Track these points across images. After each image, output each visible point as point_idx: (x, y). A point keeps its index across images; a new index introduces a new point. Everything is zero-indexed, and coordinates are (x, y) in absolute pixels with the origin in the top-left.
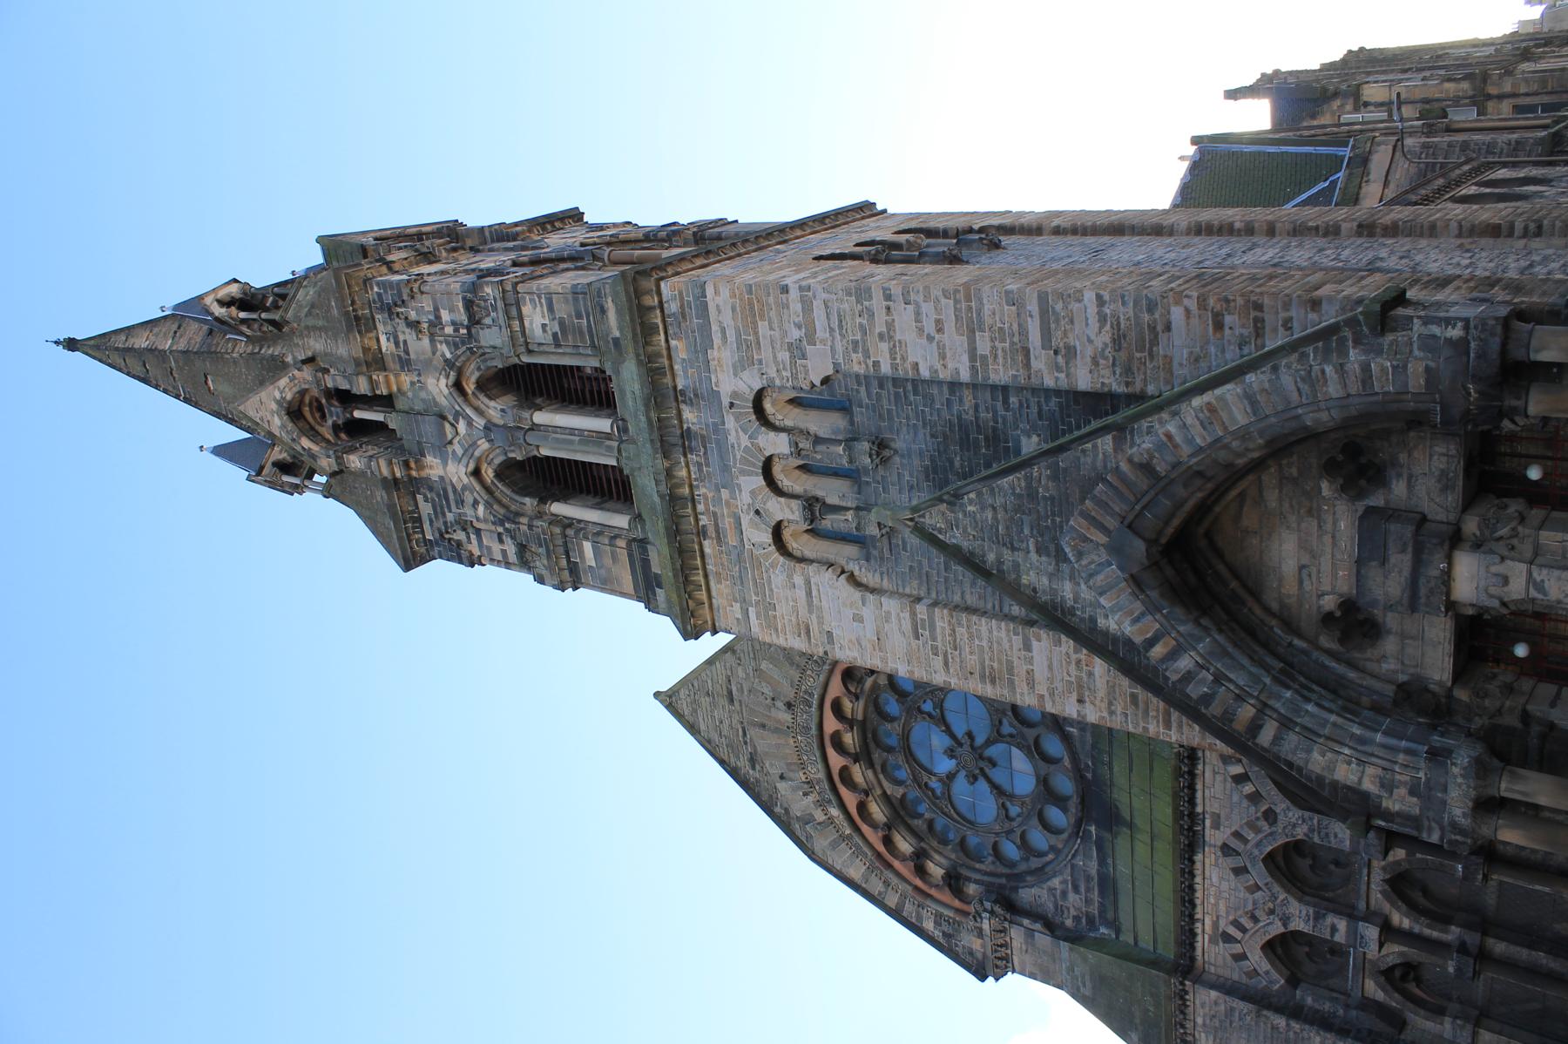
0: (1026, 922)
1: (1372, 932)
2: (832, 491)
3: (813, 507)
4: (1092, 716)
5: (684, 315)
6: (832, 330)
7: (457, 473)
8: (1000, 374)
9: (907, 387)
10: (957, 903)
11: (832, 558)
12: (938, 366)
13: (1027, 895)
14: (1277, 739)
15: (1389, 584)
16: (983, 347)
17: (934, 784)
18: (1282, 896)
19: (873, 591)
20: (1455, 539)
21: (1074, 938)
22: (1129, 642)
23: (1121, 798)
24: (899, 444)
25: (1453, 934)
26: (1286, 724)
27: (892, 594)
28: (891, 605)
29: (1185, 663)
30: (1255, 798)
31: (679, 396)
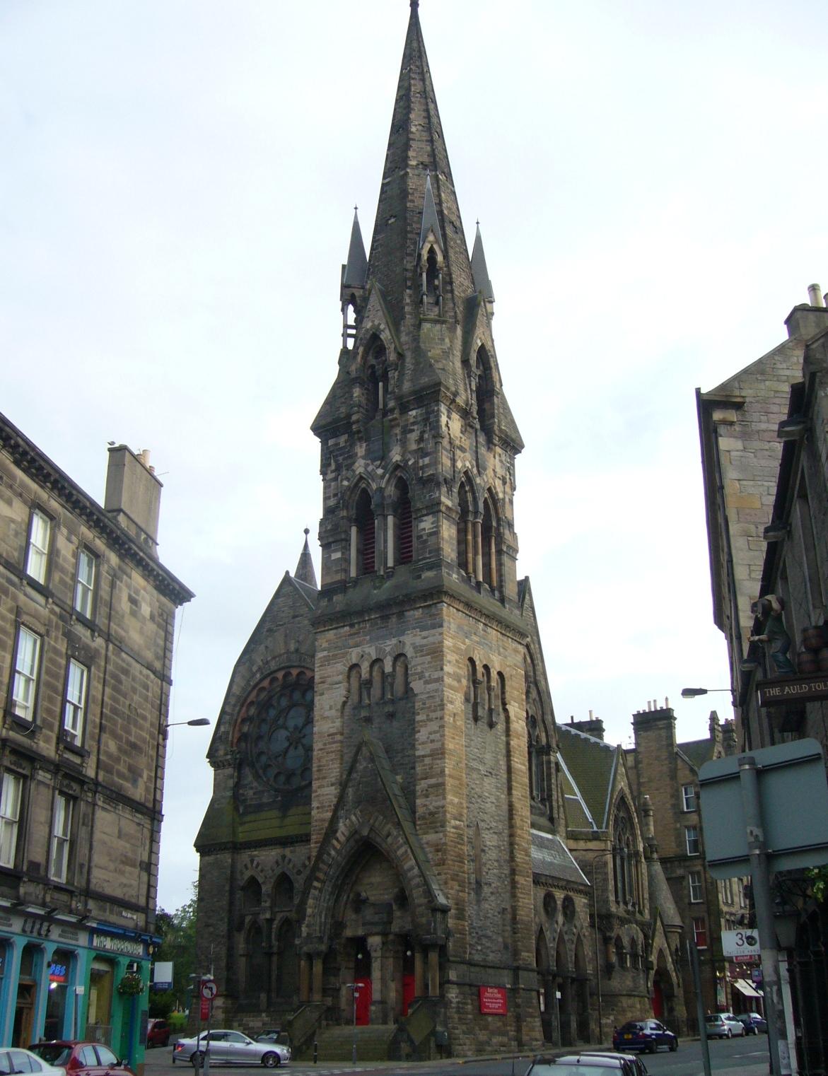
0: (236, 774)
1: (268, 916)
2: (376, 691)
3: (368, 684)
4: (314, 813)
5: (430, 616)
6: (428, 693)
7: (360, 467)
8: (419, 769)
9: (412, 728)
10: (235, 741)
11: (352, 691)
12: (420, 741)
13: (247, 771)
14: (315, 888)
15: (369, 914)
16: (427, 761)
17: (281, 722)
18: (272, 880)
19: (342, 713)
20: (384, 934)
21: (236, 797)
22: (336, 831)
23: (292, 811)
24: (395, 724)
25: (275, 943)
26: (320, 890)
27: (343, 722)
28: (338, 723)
29: (333, 853)
30: (304, 866)
31: (401, 615)
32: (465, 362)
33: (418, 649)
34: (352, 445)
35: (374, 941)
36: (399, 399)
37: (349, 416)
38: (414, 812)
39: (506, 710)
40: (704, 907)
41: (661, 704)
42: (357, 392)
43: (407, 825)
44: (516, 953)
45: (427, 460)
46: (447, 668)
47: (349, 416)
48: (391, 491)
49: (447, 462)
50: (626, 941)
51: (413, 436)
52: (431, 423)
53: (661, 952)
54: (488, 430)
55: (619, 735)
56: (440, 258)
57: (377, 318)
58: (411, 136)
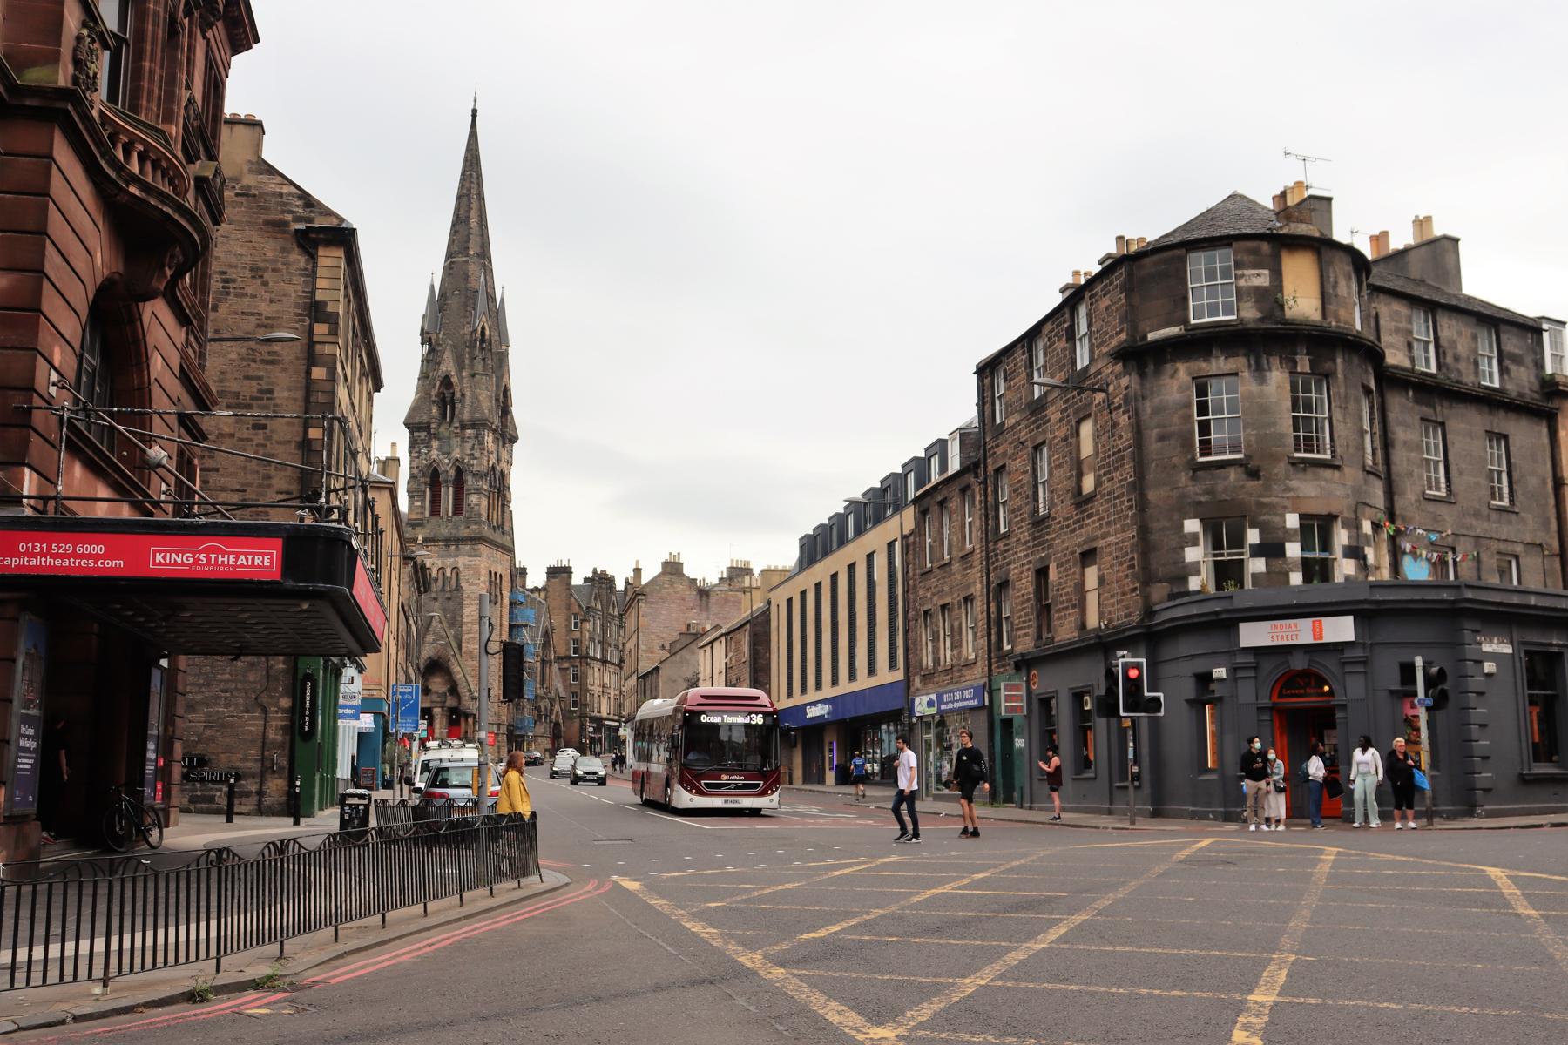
2: (440, 583)
7: (434, 454)
8: (464, 628)
15: (435, 697)
16: (469, 625)
20: (442, 707)
24: (451, 603)
31: (457, 546)
32: (497, 400)
33: (466, 567)
34: (430, 440)
35: (437, 711)
36: (461, 422)
37: (429, 424)
38: (460, 647)
39: (501, 594)
40: (578, 687)
41: (565, 563)
42: (435, 410)
43: (458, 656)
44: (499, 716)
45: (475, 462)
46: (482, 579)
47: (429, 424)
48: (452, 473)
49: (485, 463)
50: (543, 709)
51: (469, 445)
52: (479, 438)
53: (557, 713)
54: (503, 435)
55: (536, 578)
56: (487, 333)
57: (448, 366)
58: (471, 231)
